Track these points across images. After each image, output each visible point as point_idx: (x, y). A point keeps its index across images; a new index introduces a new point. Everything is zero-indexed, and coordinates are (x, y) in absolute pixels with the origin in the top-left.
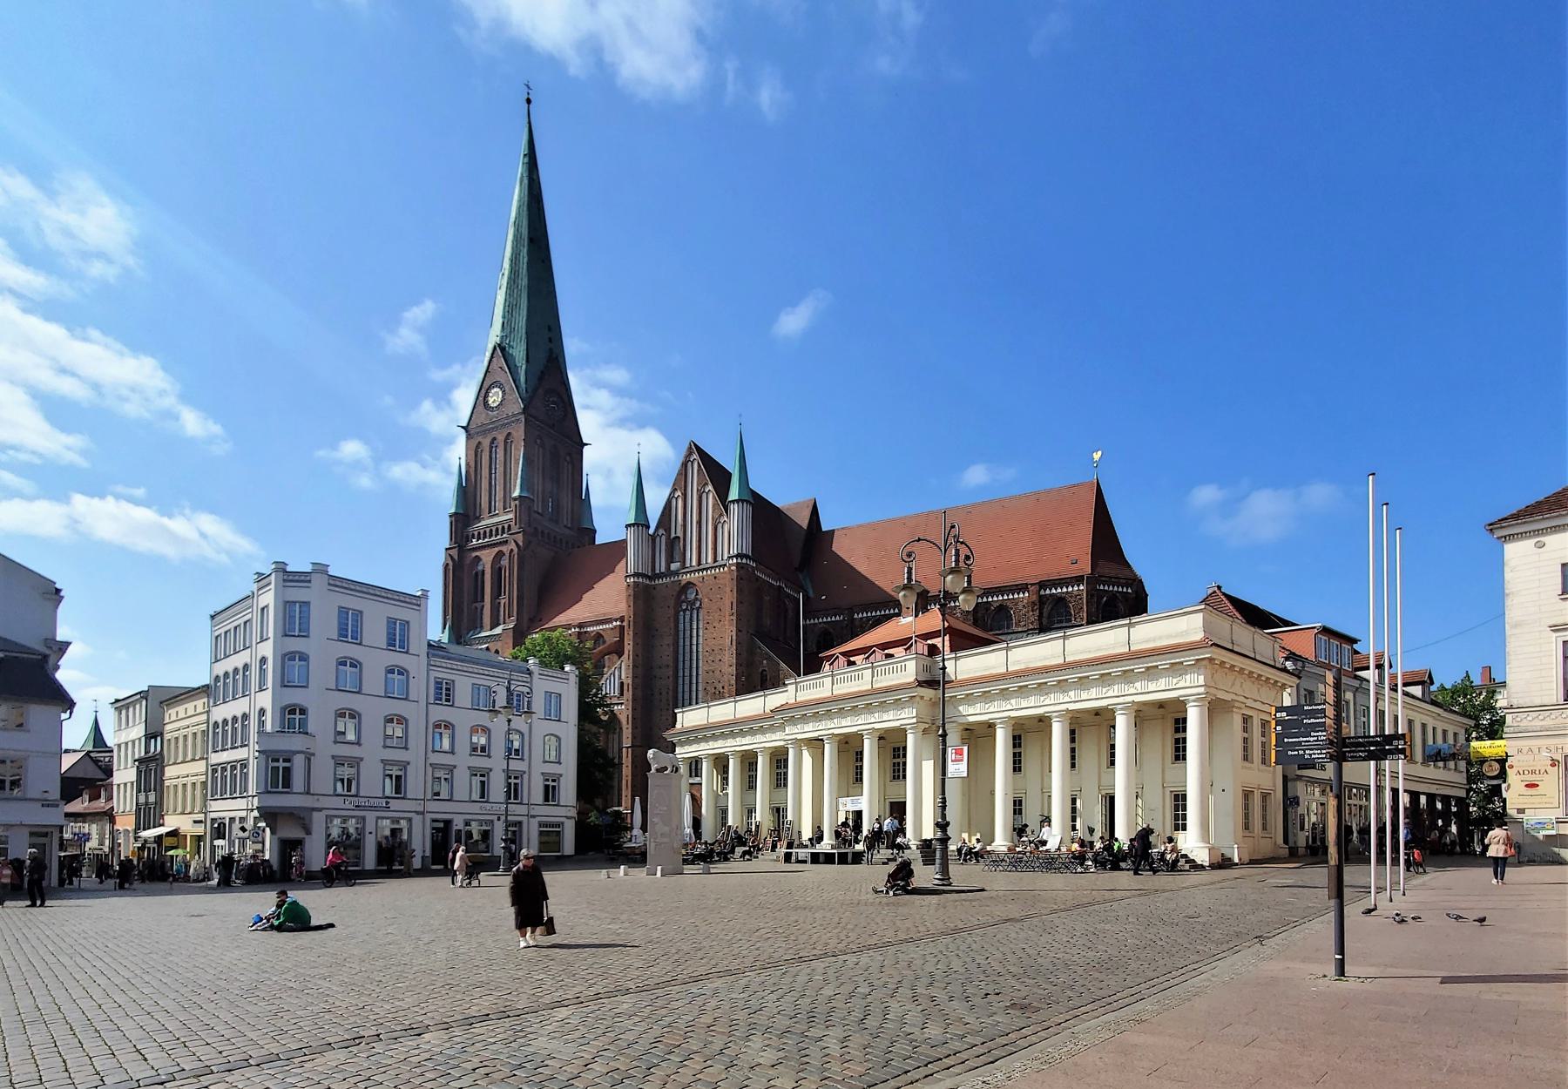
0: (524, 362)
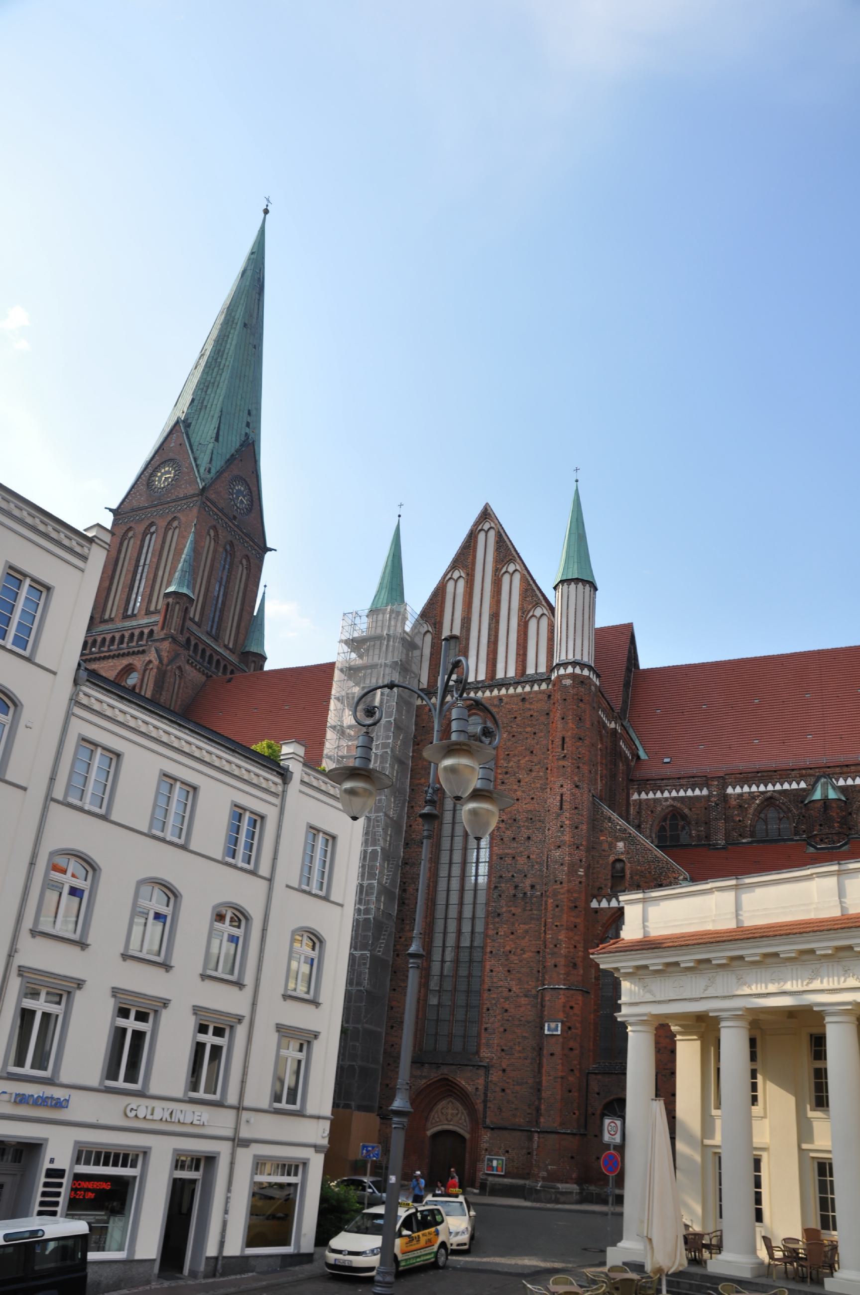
0: (213, 440)
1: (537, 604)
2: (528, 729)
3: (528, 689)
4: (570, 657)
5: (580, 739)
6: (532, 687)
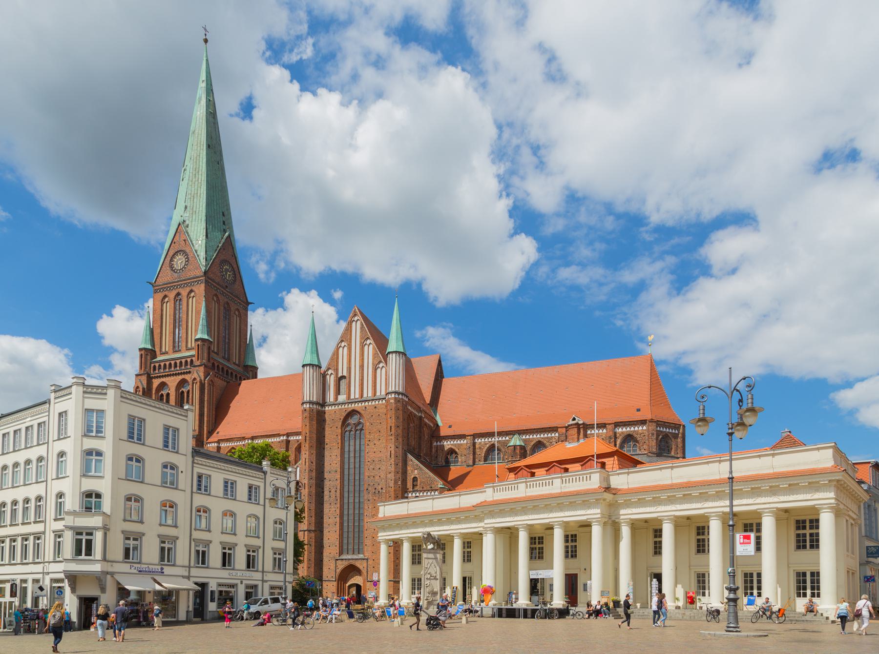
2: (378, 421)
4: (393, 389)
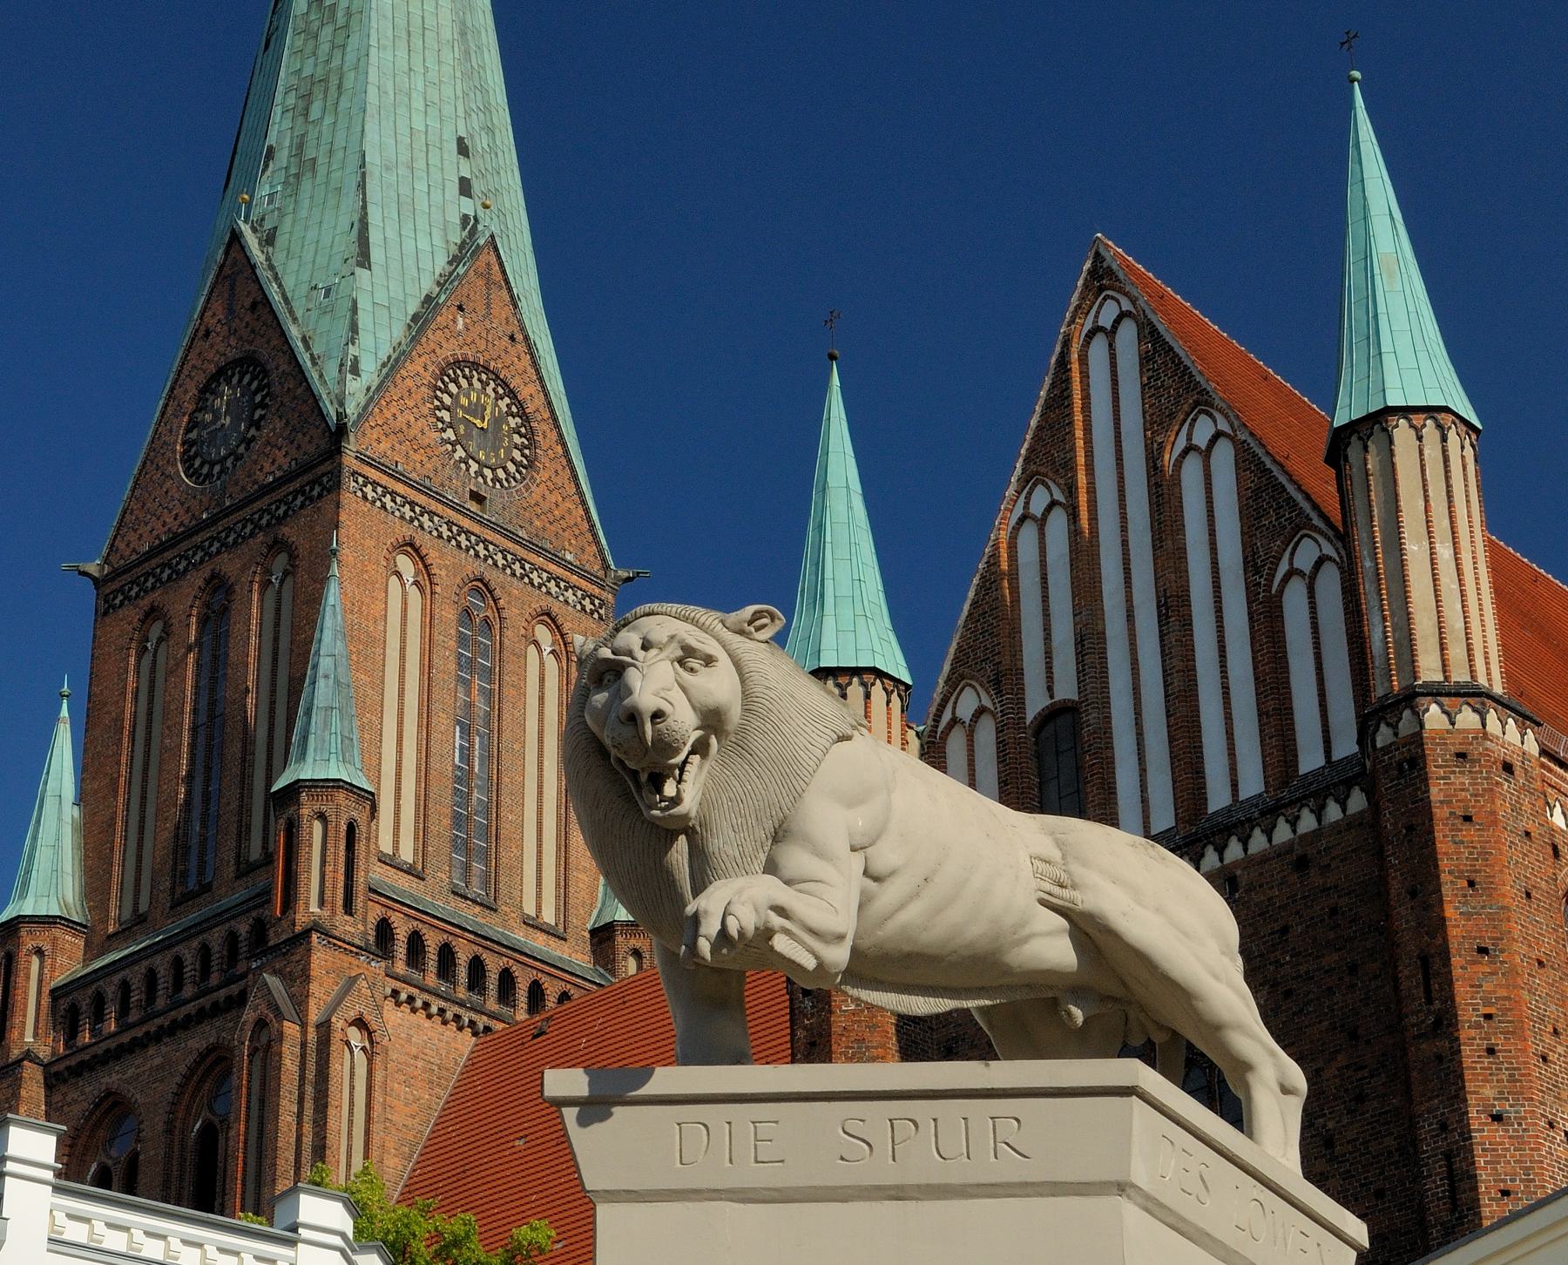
1: (1296, 528)
2: (1332, 959)
3: (1308, 822)
5: (1483, 951)
6: (1319, 813)
